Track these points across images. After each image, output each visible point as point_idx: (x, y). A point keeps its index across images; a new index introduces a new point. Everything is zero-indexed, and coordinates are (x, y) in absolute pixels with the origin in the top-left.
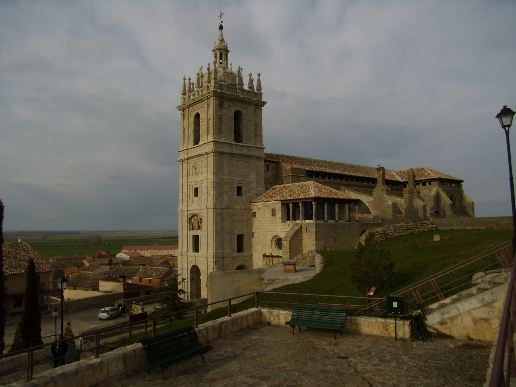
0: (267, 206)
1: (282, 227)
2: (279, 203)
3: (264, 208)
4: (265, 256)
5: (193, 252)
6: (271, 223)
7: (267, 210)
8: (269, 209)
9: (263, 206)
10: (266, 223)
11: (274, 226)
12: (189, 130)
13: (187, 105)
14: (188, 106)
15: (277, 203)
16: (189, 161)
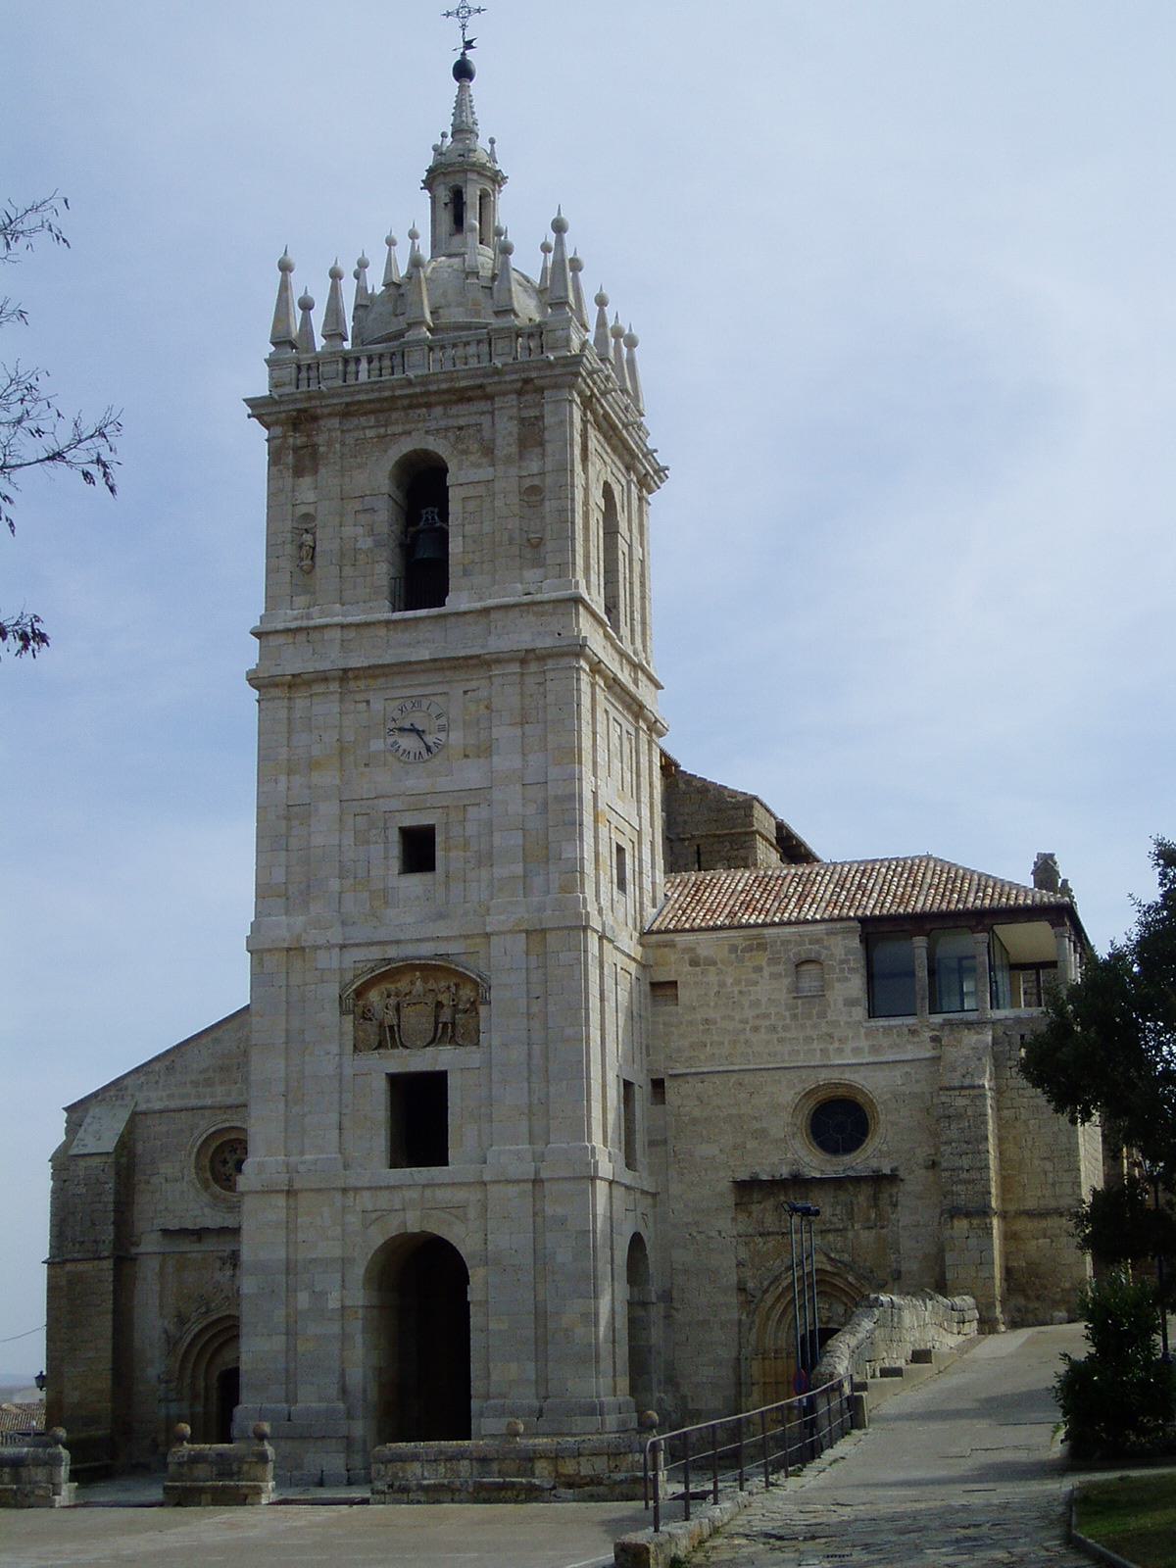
0: (762, 947)
1: (864, 1044)
2: (849, 931)
3: (741, 960)
4: (748, 1189)
5: (393, 1165)
6: (786, 1028)
7: (758, 969)
8: (772, 961)
9: (733, 949)
10: (756, 1029)
11: (809, 1039)
12: (348, 531)
13: (348, 399)
14: (347, 404)
15: (830, 933)
16: (352, 685)
